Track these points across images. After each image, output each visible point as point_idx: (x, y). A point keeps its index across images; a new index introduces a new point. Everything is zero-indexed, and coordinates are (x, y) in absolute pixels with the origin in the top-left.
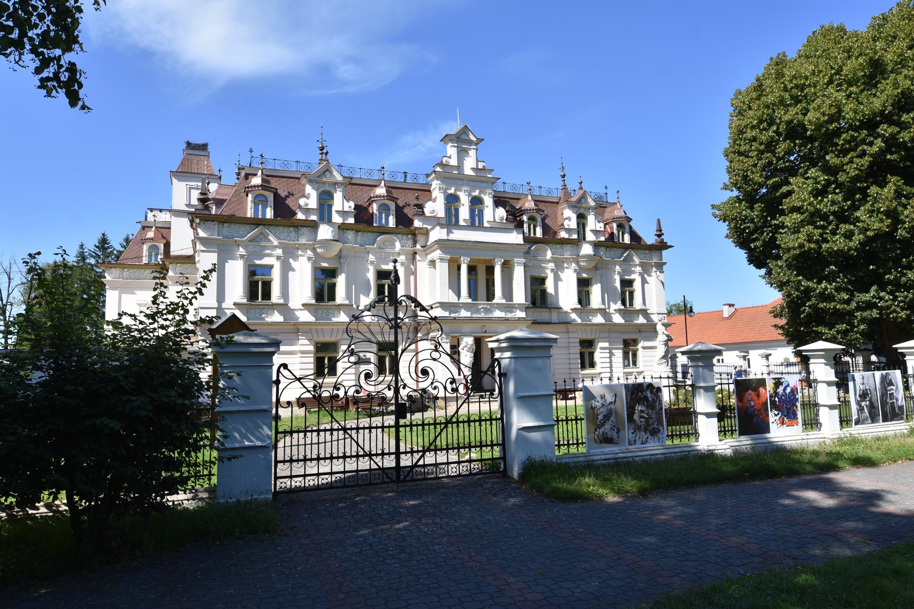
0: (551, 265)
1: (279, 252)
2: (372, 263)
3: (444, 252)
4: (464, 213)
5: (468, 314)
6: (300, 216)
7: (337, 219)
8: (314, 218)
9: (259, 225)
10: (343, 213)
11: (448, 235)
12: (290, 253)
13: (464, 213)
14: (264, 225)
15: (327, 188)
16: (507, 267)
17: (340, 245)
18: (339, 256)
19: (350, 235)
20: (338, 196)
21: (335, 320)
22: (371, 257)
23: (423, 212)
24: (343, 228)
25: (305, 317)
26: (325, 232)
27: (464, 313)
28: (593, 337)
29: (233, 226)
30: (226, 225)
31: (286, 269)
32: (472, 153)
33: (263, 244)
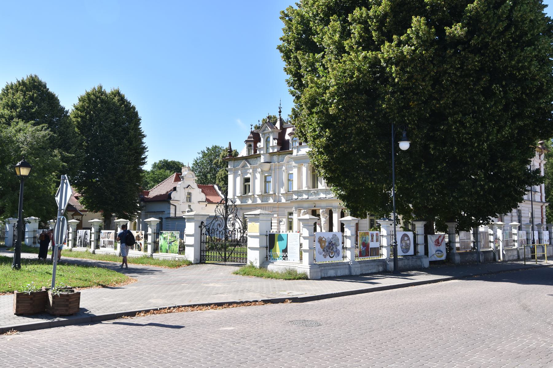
1: (251, 171)
2: (284, 171)
3: (295, 163)
5: (307, 197)
6: (258, 152)
7: (271, 151)
10: (273, 147)
12: (255, 171)
18: (270, 169)
19: (275, 158)
20: (271, 138)
21: (269, 202)
22: (284, 168)
24: (272, 154)
25: (259, 201)
27: (305, 196)
31: (255, 178)
33: (246, 168)
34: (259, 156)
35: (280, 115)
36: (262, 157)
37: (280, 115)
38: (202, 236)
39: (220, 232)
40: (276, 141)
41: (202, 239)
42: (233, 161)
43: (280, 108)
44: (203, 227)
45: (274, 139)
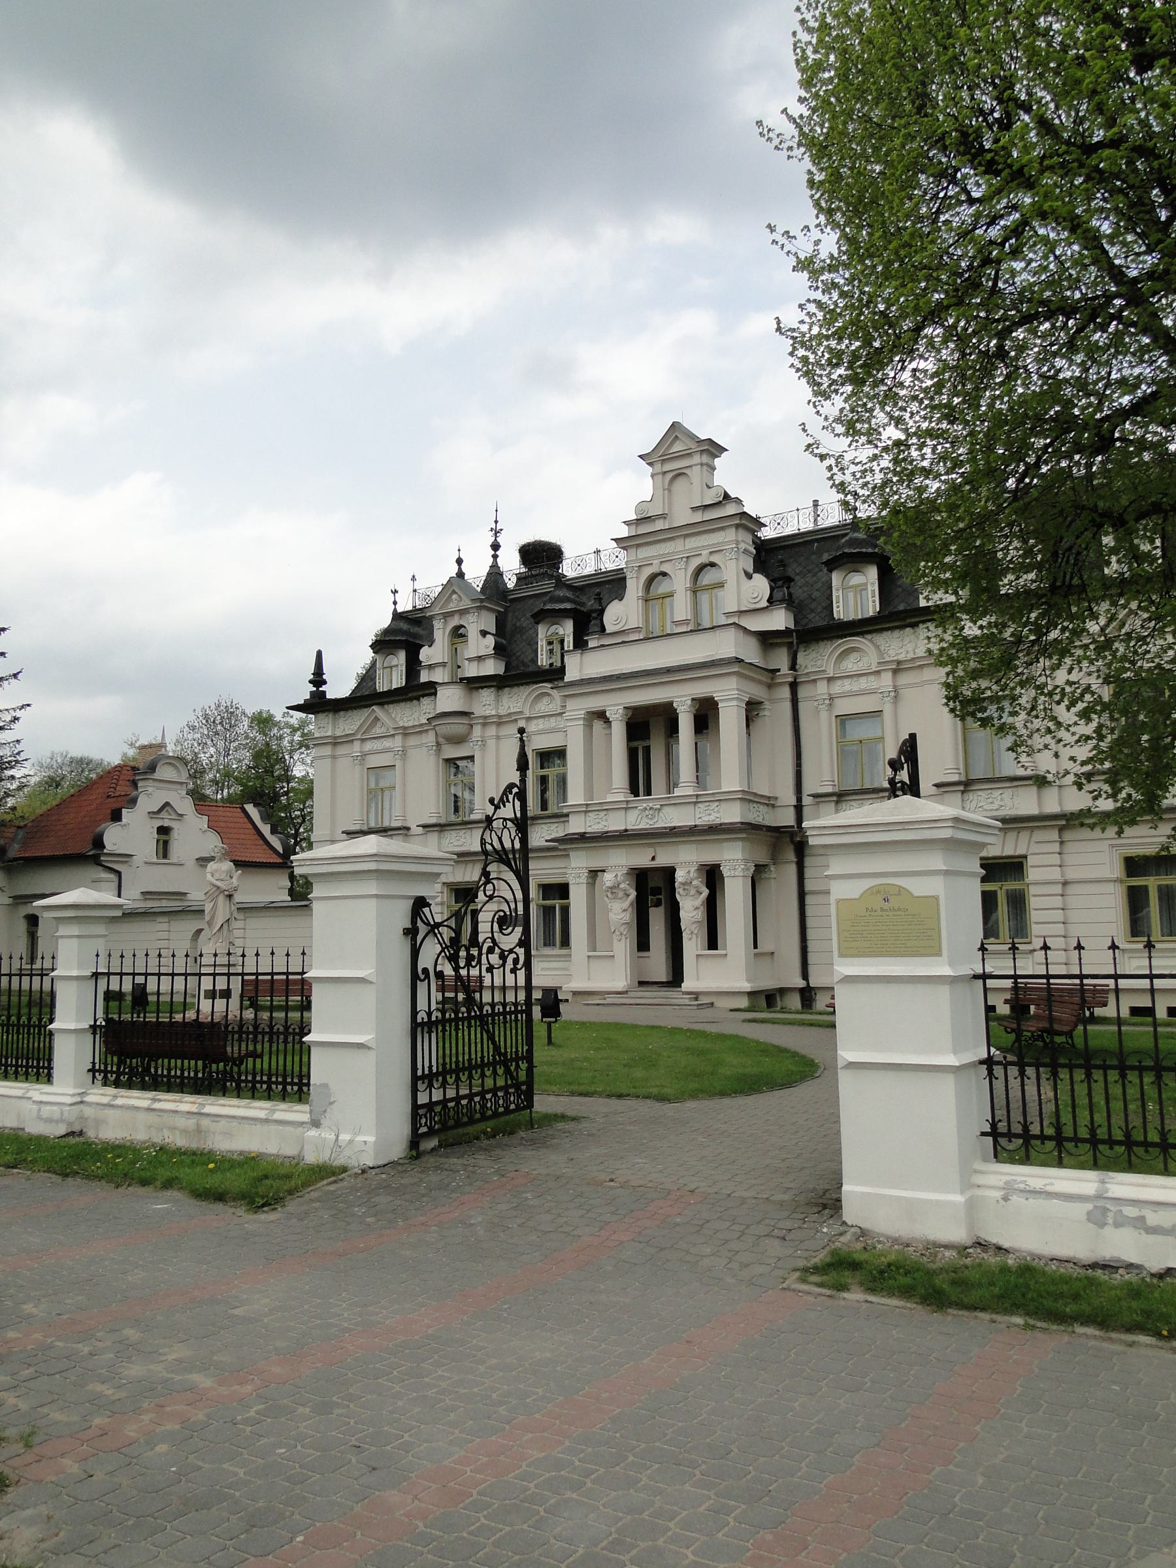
0: (887, 680)
4: (681, 608)
6: (424, 677)
7: (472, 671)
8: (438, 676)
9: (370, 706)
11: (581, 670)
13: (681, 608)
14: (381, 704)
15: (455, 621)
16: (706, 716)
17: (464, 720)
20: (473, 631)
23: (603, 629)
24: (474, 684)
26: (449, 699)
28: (1009, 851)
29: (350, 713)
30: (342, 713)
32: (695, 474)
34: (431, 689)
35: (495, 557)
36: (441, 692)
37: (495, 557)
38: (422, 988)
39: (503, 957)
40: (490, 641)
41: (422, 1005)
42: (331, 715)
43: (497, 532)
44: (423, 929)
45: (484, 633)
